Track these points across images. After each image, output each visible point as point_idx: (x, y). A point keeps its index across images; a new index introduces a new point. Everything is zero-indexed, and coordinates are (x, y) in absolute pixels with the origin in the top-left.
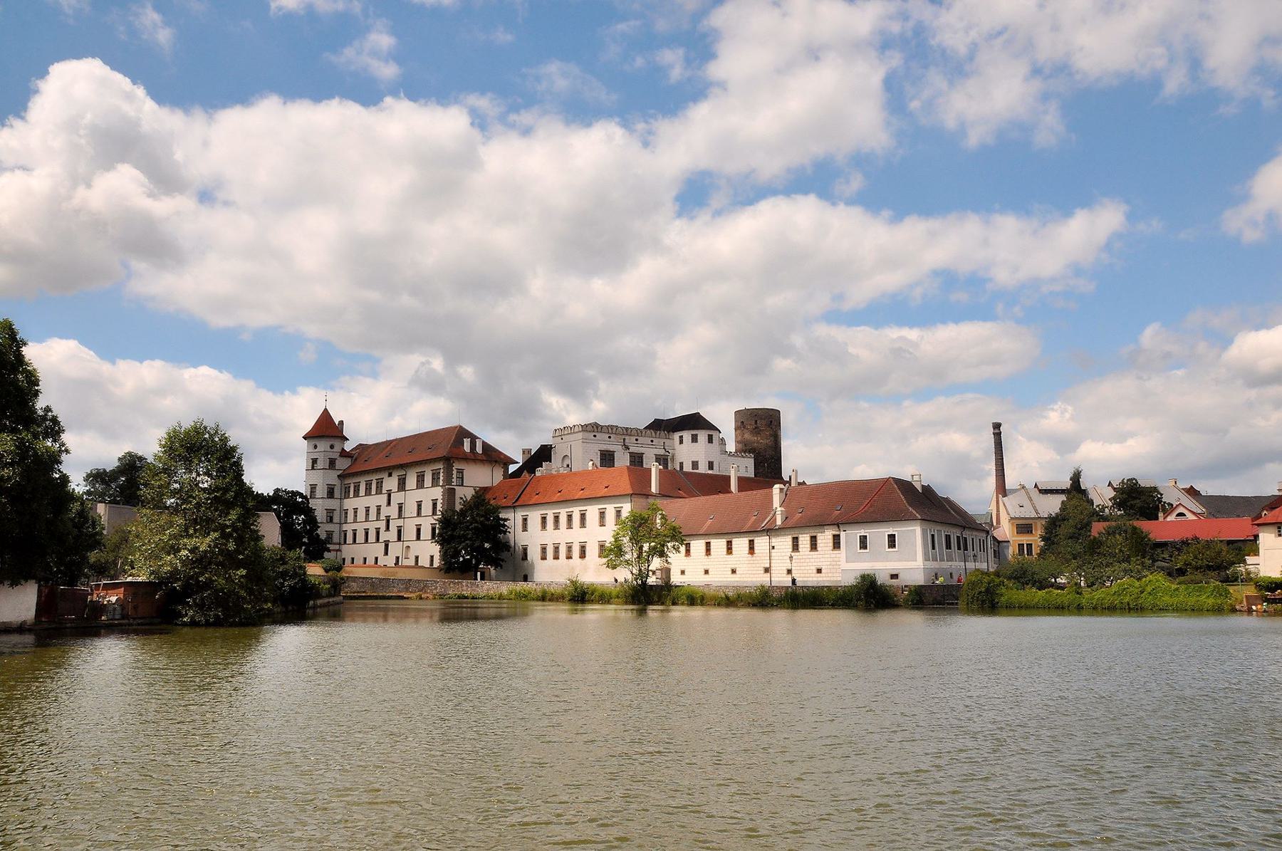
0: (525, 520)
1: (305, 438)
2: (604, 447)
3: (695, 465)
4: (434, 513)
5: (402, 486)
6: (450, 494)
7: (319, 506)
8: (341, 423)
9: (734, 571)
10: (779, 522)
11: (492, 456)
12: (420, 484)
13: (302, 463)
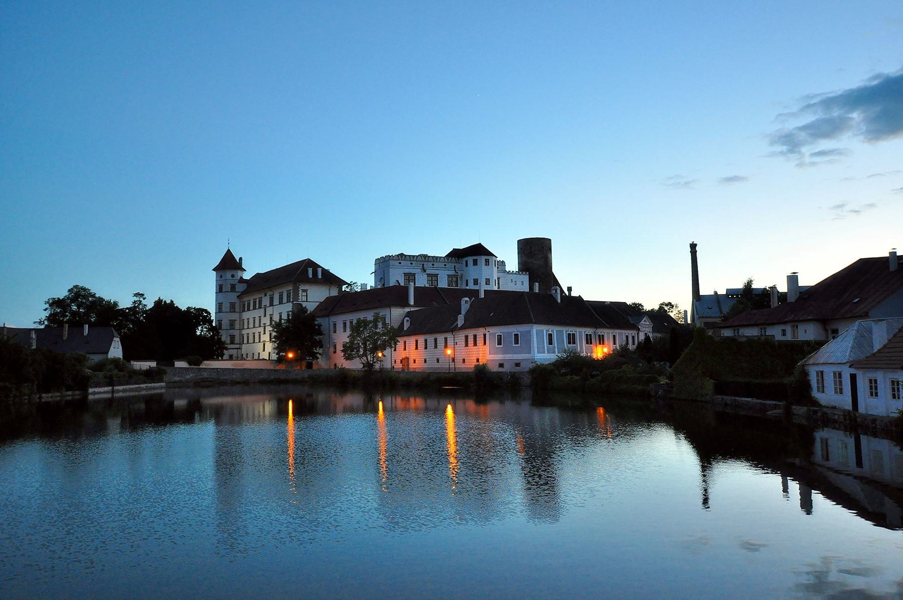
2: (407, 271)
5: (271, 304)
8: (241, 259)
12: (281, 302)
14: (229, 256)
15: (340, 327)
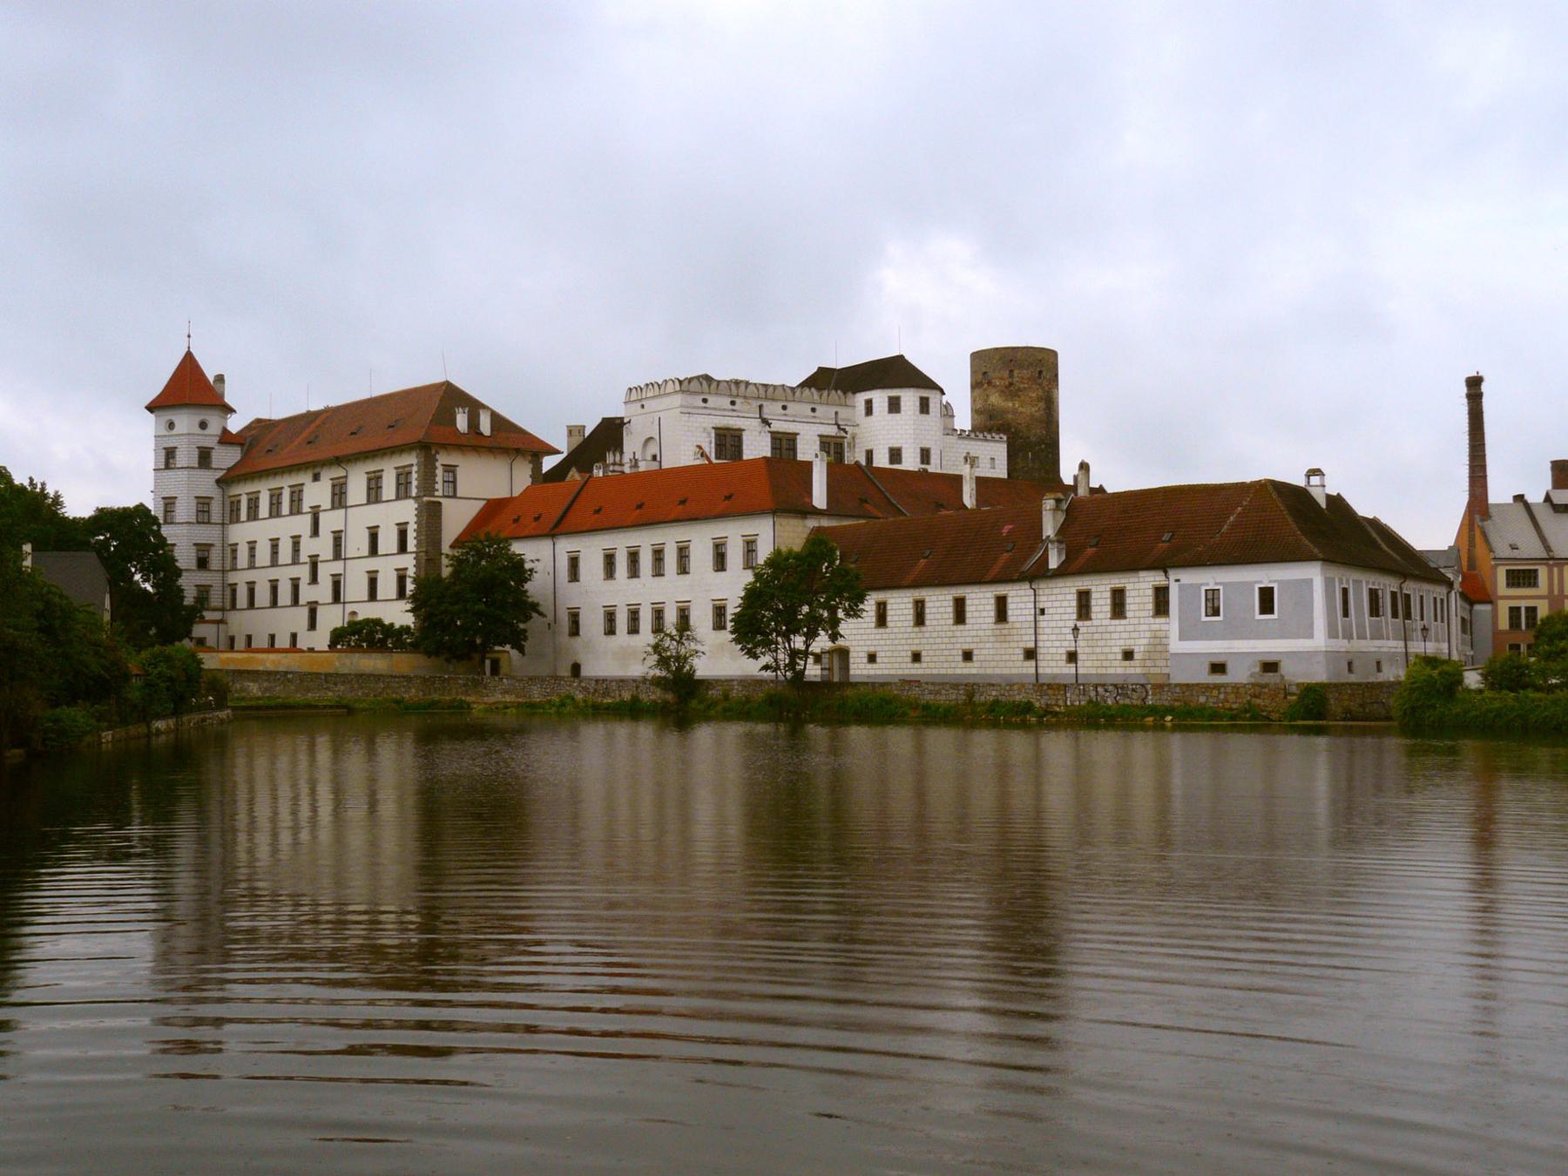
0: (574, 563)
1: (151, 408)
3: (895, 455)
4: (403, 548)
5: (339, 498)
6: (431, 515)
7: (181, 539)
8: (220, 379)
9: (968, 656)
10: (1053, 563)
11: (510, 441)
13: (146, 457)
14: (189, 368)
15: (592, 565)
